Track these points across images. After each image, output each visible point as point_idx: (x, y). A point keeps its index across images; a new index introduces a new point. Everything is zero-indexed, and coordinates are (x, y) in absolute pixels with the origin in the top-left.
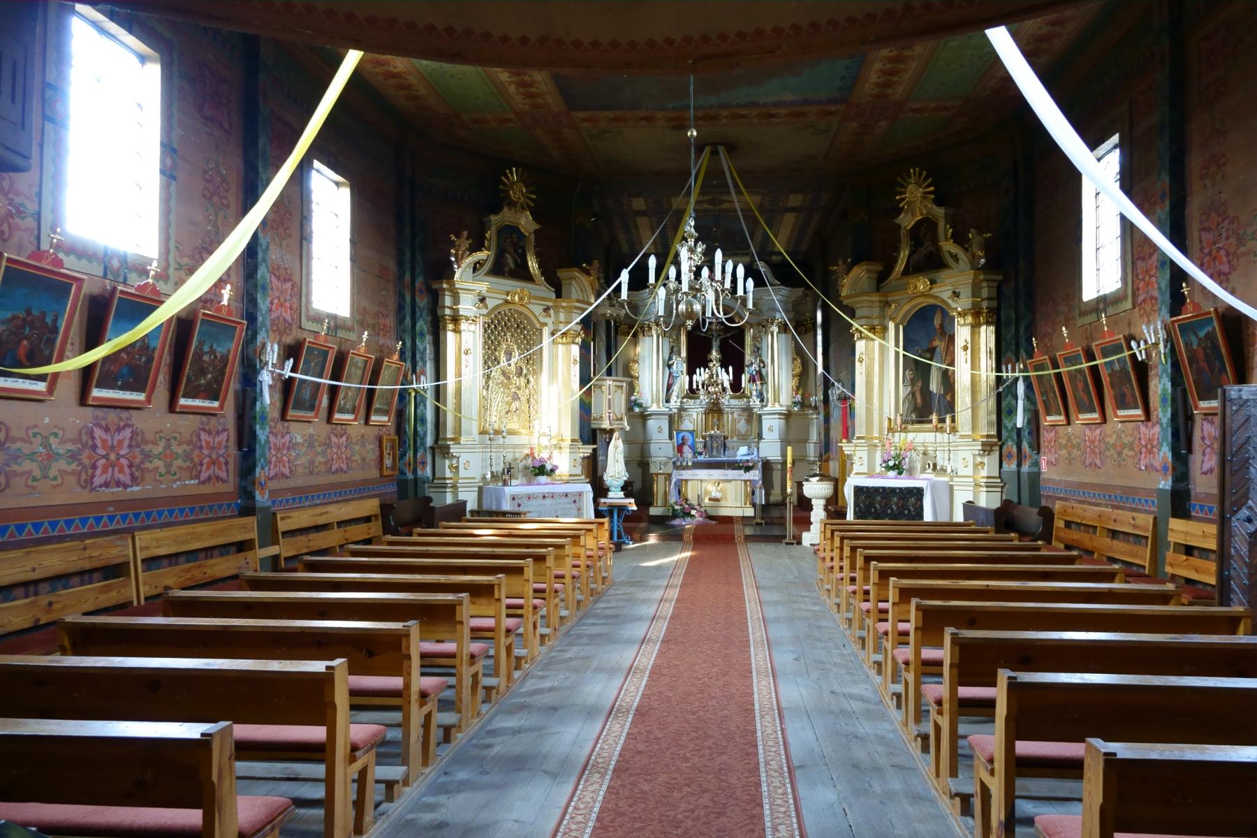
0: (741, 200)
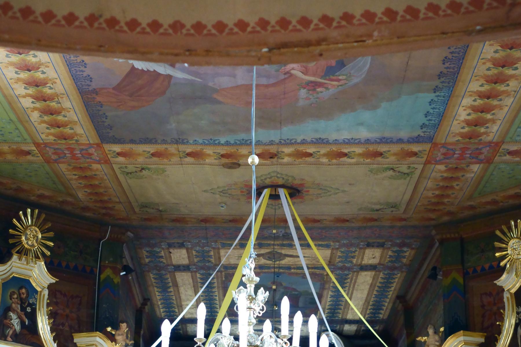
0: (307, 255)
